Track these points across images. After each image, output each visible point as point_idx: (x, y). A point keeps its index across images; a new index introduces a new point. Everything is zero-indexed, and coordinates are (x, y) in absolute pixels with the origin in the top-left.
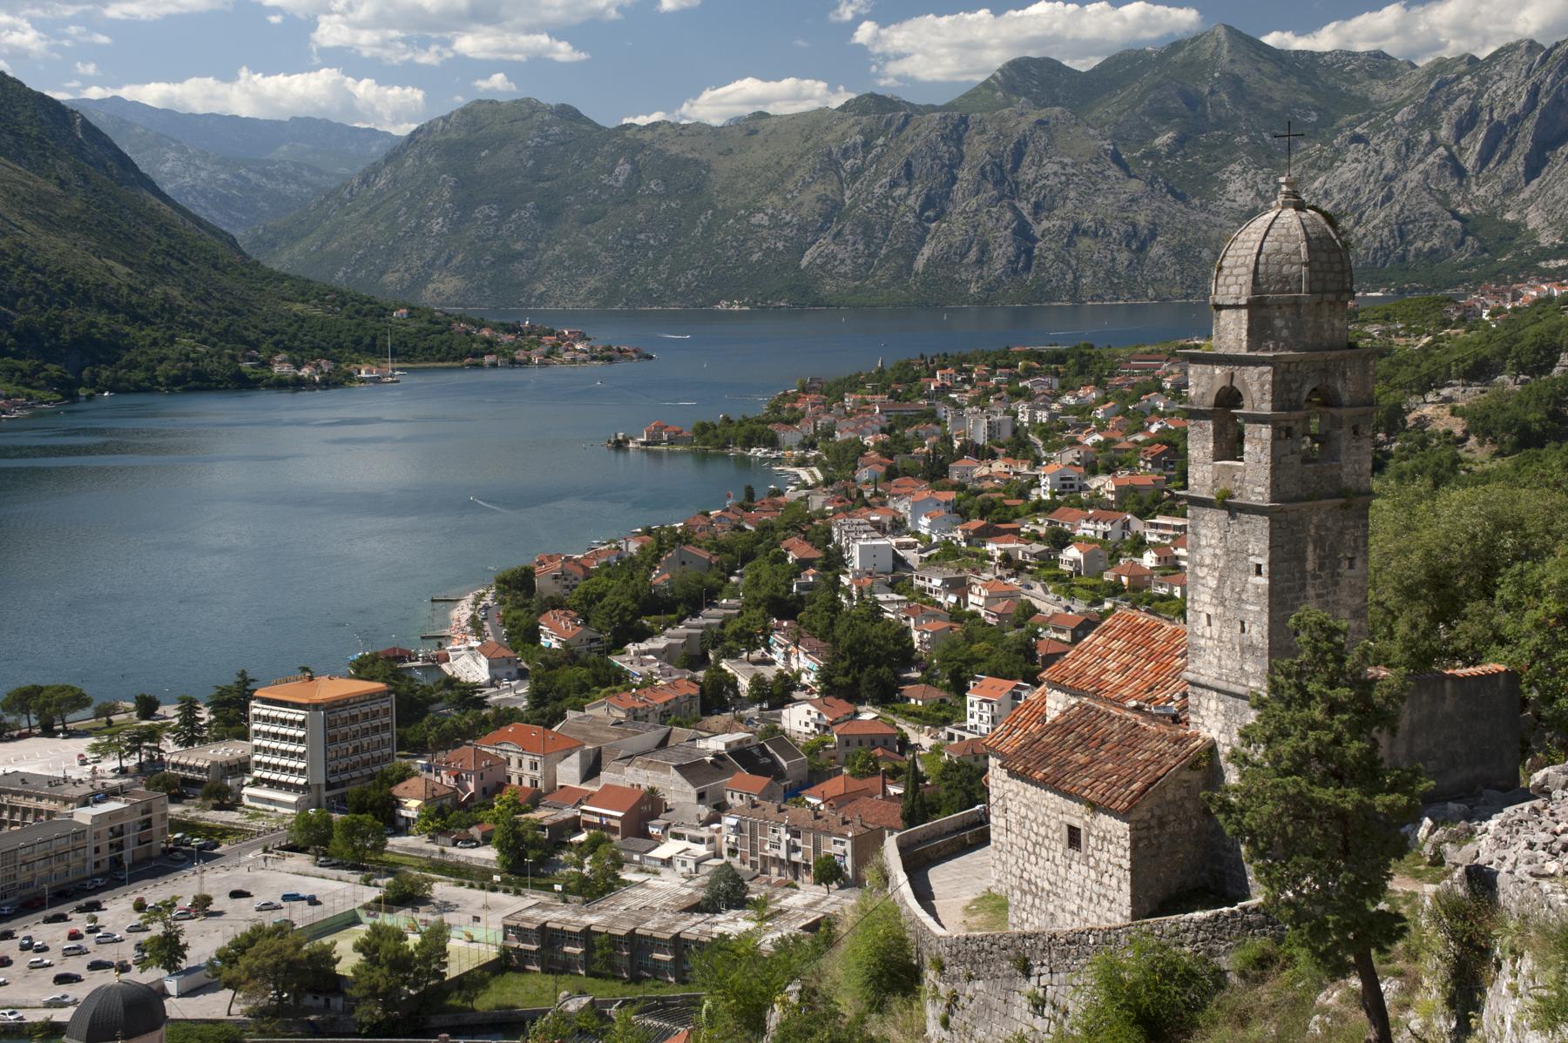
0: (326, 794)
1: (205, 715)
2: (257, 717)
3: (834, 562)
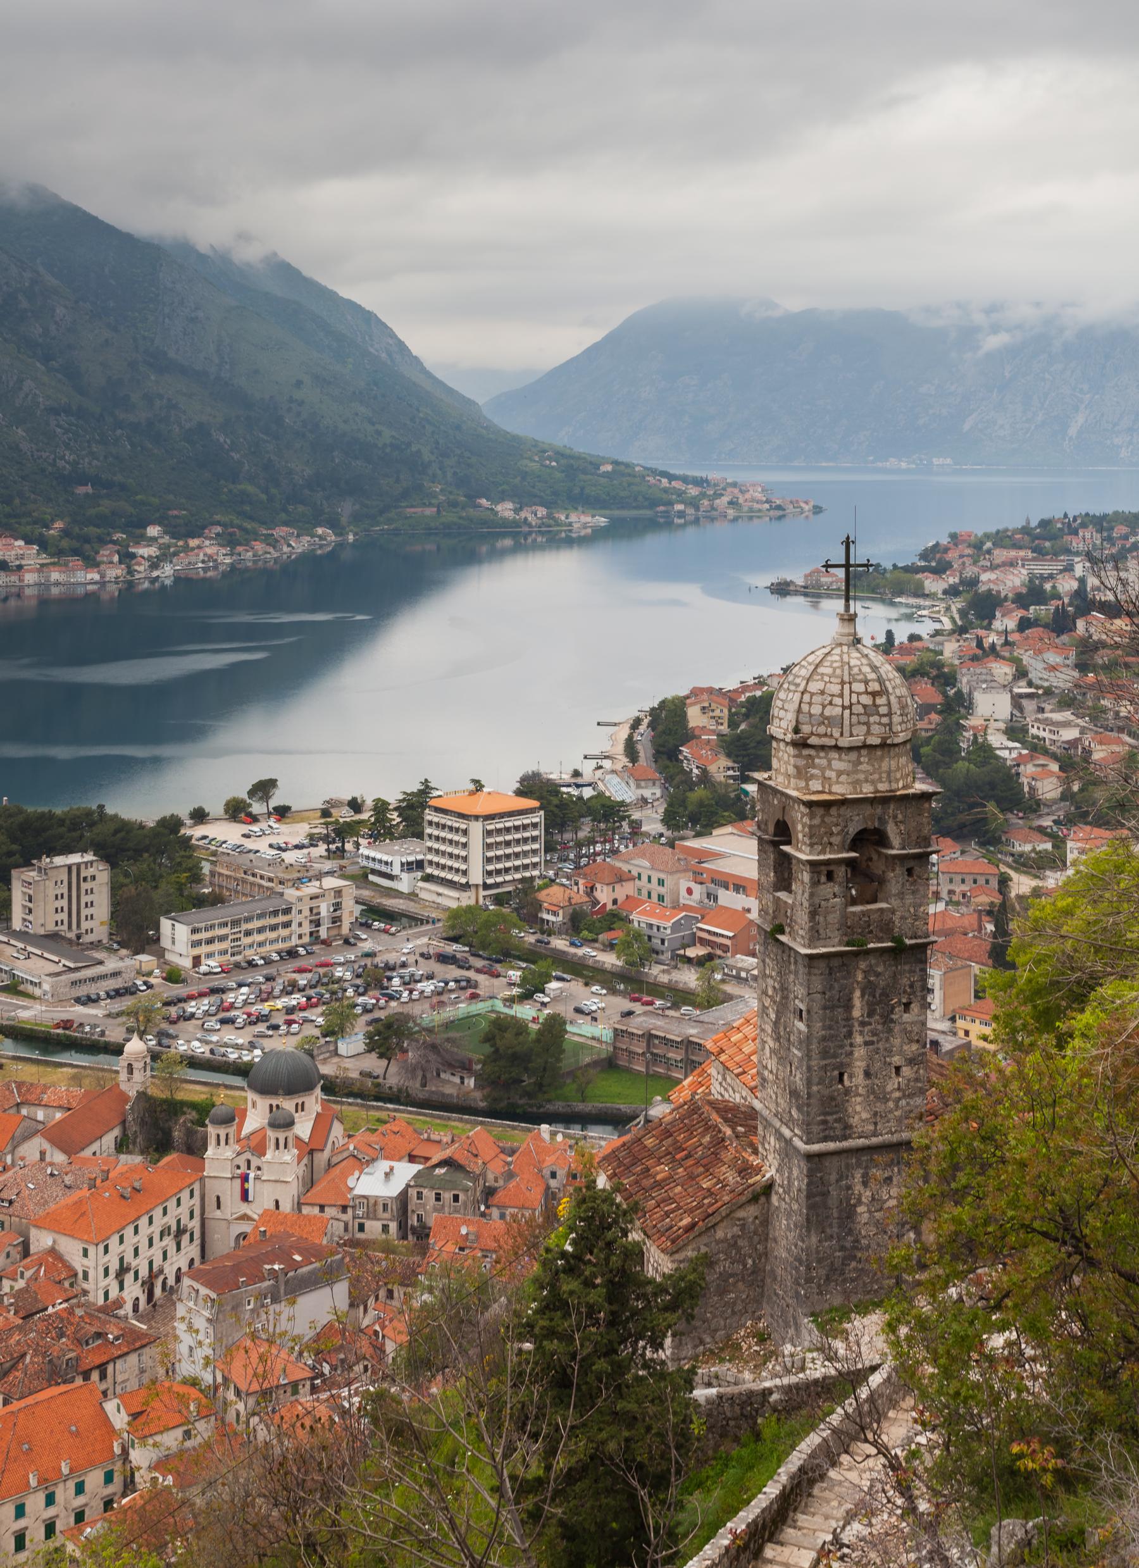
0: (482, 893)
2: (430, 823)
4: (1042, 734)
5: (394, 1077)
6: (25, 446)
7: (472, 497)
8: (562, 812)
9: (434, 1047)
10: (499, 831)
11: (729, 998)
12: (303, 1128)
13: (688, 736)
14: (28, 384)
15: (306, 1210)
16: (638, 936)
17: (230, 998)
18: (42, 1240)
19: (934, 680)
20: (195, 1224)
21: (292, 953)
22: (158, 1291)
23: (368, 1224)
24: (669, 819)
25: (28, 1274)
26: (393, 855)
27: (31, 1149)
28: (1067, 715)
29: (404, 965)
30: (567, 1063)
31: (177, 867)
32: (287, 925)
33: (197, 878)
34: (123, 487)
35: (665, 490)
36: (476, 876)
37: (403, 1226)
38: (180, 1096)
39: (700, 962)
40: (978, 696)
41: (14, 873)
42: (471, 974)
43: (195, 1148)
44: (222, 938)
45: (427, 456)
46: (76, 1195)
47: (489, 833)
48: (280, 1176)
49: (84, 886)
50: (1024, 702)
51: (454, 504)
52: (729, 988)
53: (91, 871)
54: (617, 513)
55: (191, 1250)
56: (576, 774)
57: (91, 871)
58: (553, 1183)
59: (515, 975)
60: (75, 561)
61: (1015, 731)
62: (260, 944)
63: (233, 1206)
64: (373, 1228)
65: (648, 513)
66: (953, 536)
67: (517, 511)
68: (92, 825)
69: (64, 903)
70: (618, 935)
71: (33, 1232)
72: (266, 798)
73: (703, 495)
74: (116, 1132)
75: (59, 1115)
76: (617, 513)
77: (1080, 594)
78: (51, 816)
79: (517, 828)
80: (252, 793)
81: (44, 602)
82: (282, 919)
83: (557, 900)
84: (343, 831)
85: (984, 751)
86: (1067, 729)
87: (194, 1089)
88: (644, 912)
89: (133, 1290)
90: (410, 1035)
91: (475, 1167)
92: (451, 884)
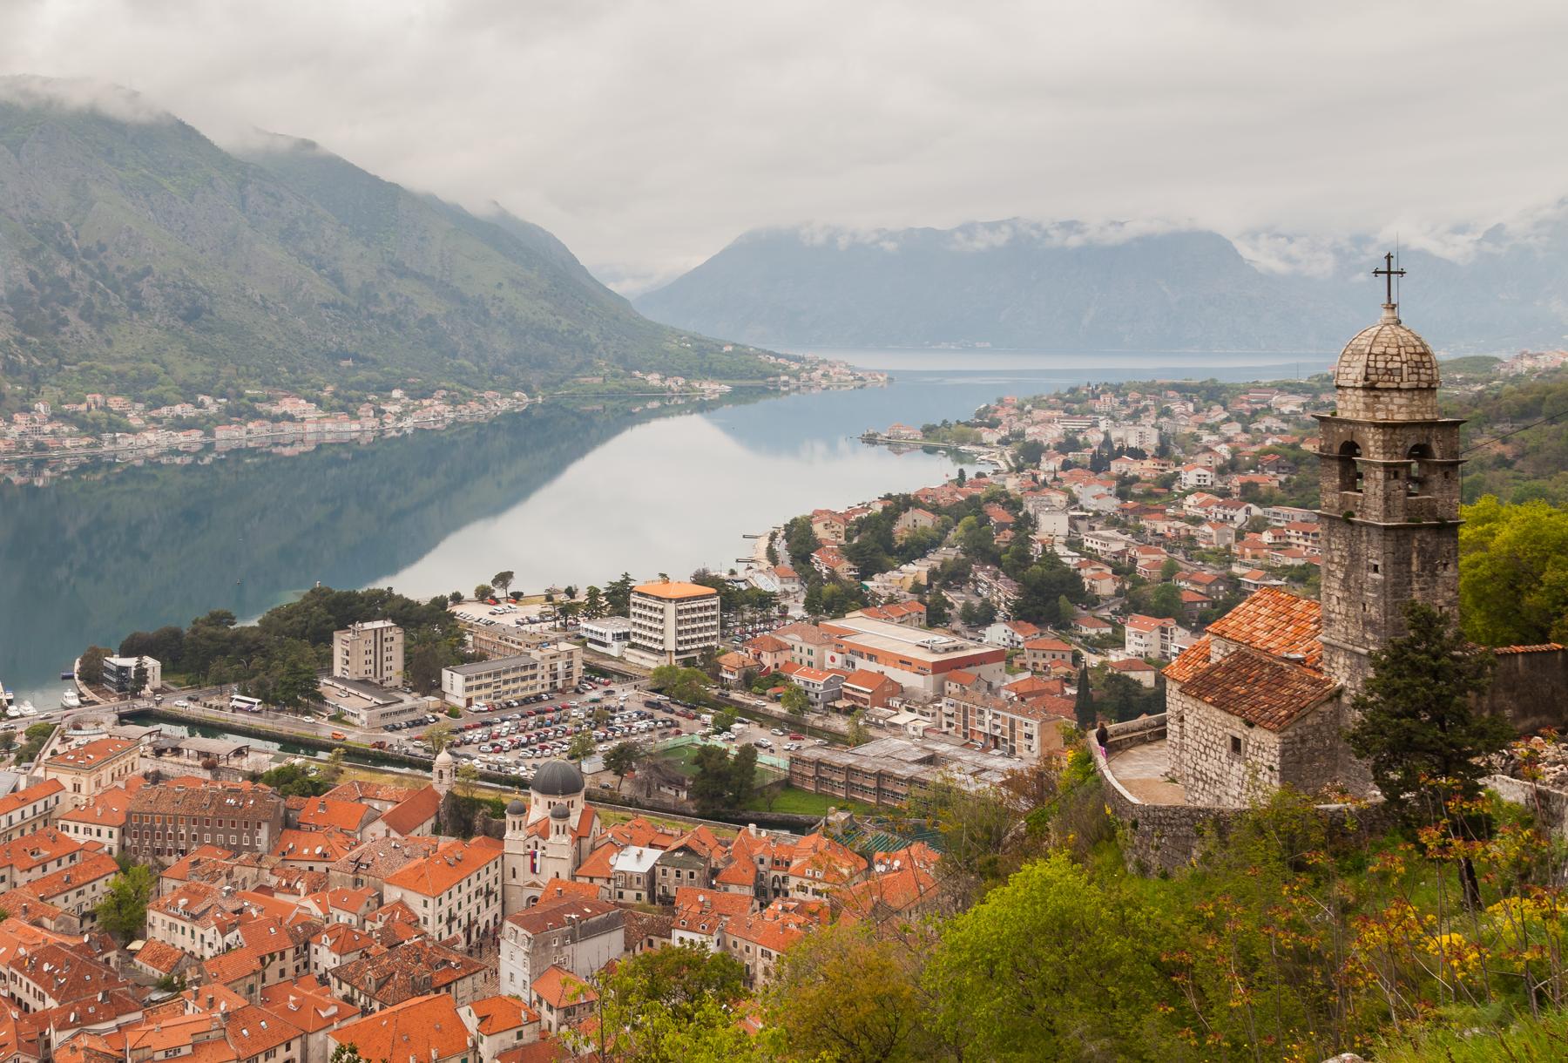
0: (675, 657)
3: (1026, 524)
4: (1095, 546)
5: (627, 789)
6: (305, 331)
7: (629, 370)
8: (733, 600)
9: (656, 767)
10: (687, 611)
11: (869, 739)
12: (574, 820)
13: (817, 545)
14: (306, 285)
15: (579, 880)
16: (798, 691)
17: (496, 729)
18: (392, 894)
19: (1004, 506)
20: (498, 888)
21: (538, 698)
22: (474, 936)
23: (626, 893)
24: (810, 606)
25: (384, 918)
26: (607, 627)
27: (379, 828)
28: (1112, 533)
29: (622, 709)
30: (757, 783)
31: (447, 634)
32: (533, 677)
33: (463, 643)
34: (374, 361)
35: (774, 366)
36: (671, 645)
37: (652, 895)
38: (476, 796)
39: (848, 712)
40: (1042, 518)
41: (336, 634)
42: (673, 716)
43: (499, 834)
44: (487, 686)
45: (594, 339)
46: (413, 864)
47: (680, 612)
48: (558, 855)
49: (386, 645)
50: (1079, 523)
51: (616, 375)
52: (872, 732)
53: (391, 634)
54: (737, 383)
55: (496, 908)
56: (733, 572)
57: (391, 634)
58: (761, 867)
59: (708, 718)
60: (343, 416)
61: (1074, 544)
62: (515, 691)
63: (525, 876)
64: (630, 896)
65: (760, 382)
66: (1000, 401)
67: (662, 380)
68: (383, 602)
69: (371, 657)
70: (782, 690)
71: (386, 888)
72: (505, 585)
73: (803, 369)
74: (432, 820)
75: (390, 807)
76: (737, 383)
77: (1107, 442)
78: (355, 595)
79: (700, 609)
80: (495, 582)
81: (319, 447)
82: (529, 672)
83: (733, 660)
84: (566, 610)
85: (1051, 559)
86: (1111, 542)
87: (486, 793)
88: (801, 673)
89: (457, 931)
90: (638, 759)
91: (704, 852)
92: (651, 650)
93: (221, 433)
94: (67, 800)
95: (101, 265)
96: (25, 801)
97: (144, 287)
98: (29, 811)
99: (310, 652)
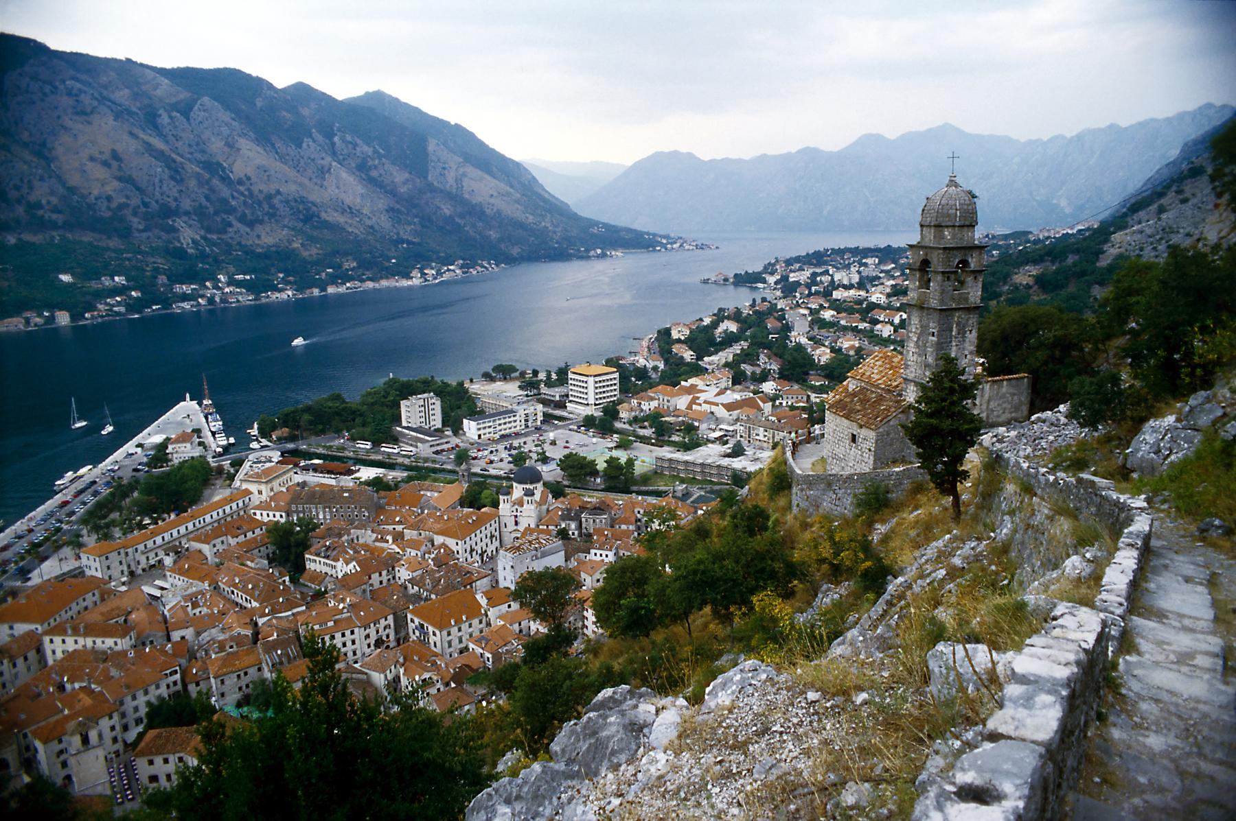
1: (554, 376)
12: (537, 497)
20: (497, 534)
36: (592, 401)
43: (496, 505)
55: (496, 544)
93: (331, 290)
94: (256, 499)
95: (249, 190)
96: (232, 501)
97: (275, 201)
98: (234, 506)
99: (389, 413)
